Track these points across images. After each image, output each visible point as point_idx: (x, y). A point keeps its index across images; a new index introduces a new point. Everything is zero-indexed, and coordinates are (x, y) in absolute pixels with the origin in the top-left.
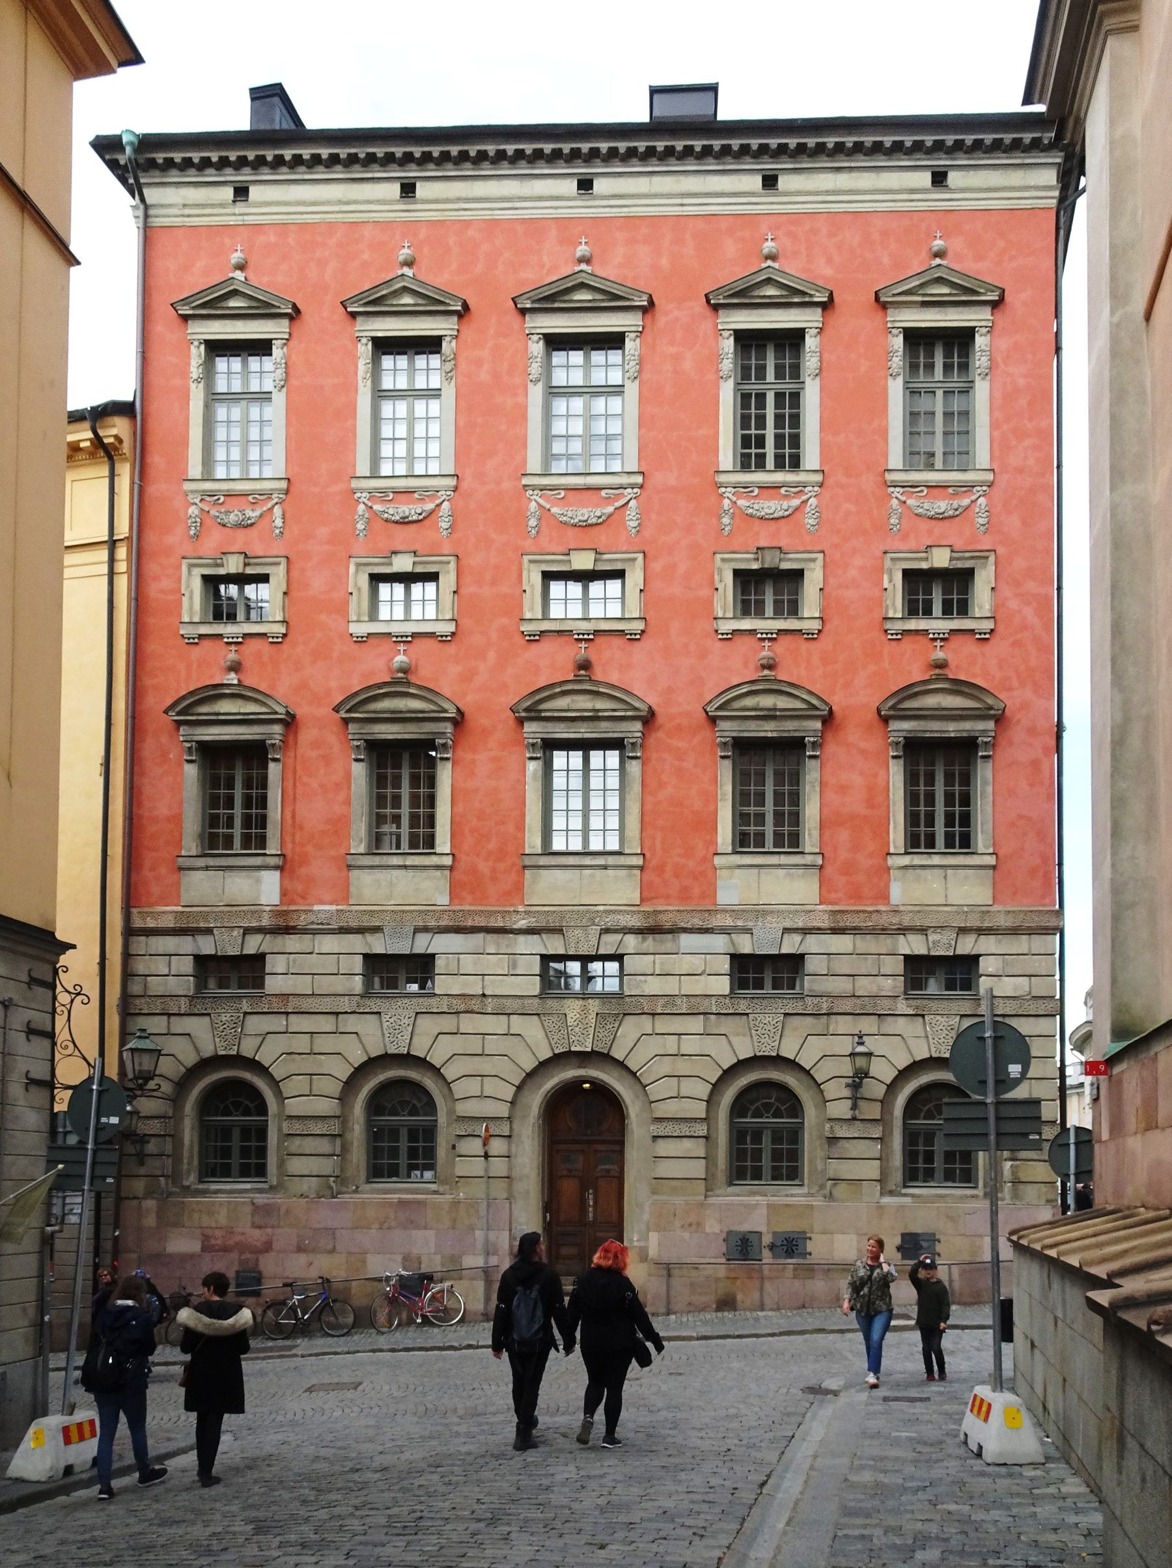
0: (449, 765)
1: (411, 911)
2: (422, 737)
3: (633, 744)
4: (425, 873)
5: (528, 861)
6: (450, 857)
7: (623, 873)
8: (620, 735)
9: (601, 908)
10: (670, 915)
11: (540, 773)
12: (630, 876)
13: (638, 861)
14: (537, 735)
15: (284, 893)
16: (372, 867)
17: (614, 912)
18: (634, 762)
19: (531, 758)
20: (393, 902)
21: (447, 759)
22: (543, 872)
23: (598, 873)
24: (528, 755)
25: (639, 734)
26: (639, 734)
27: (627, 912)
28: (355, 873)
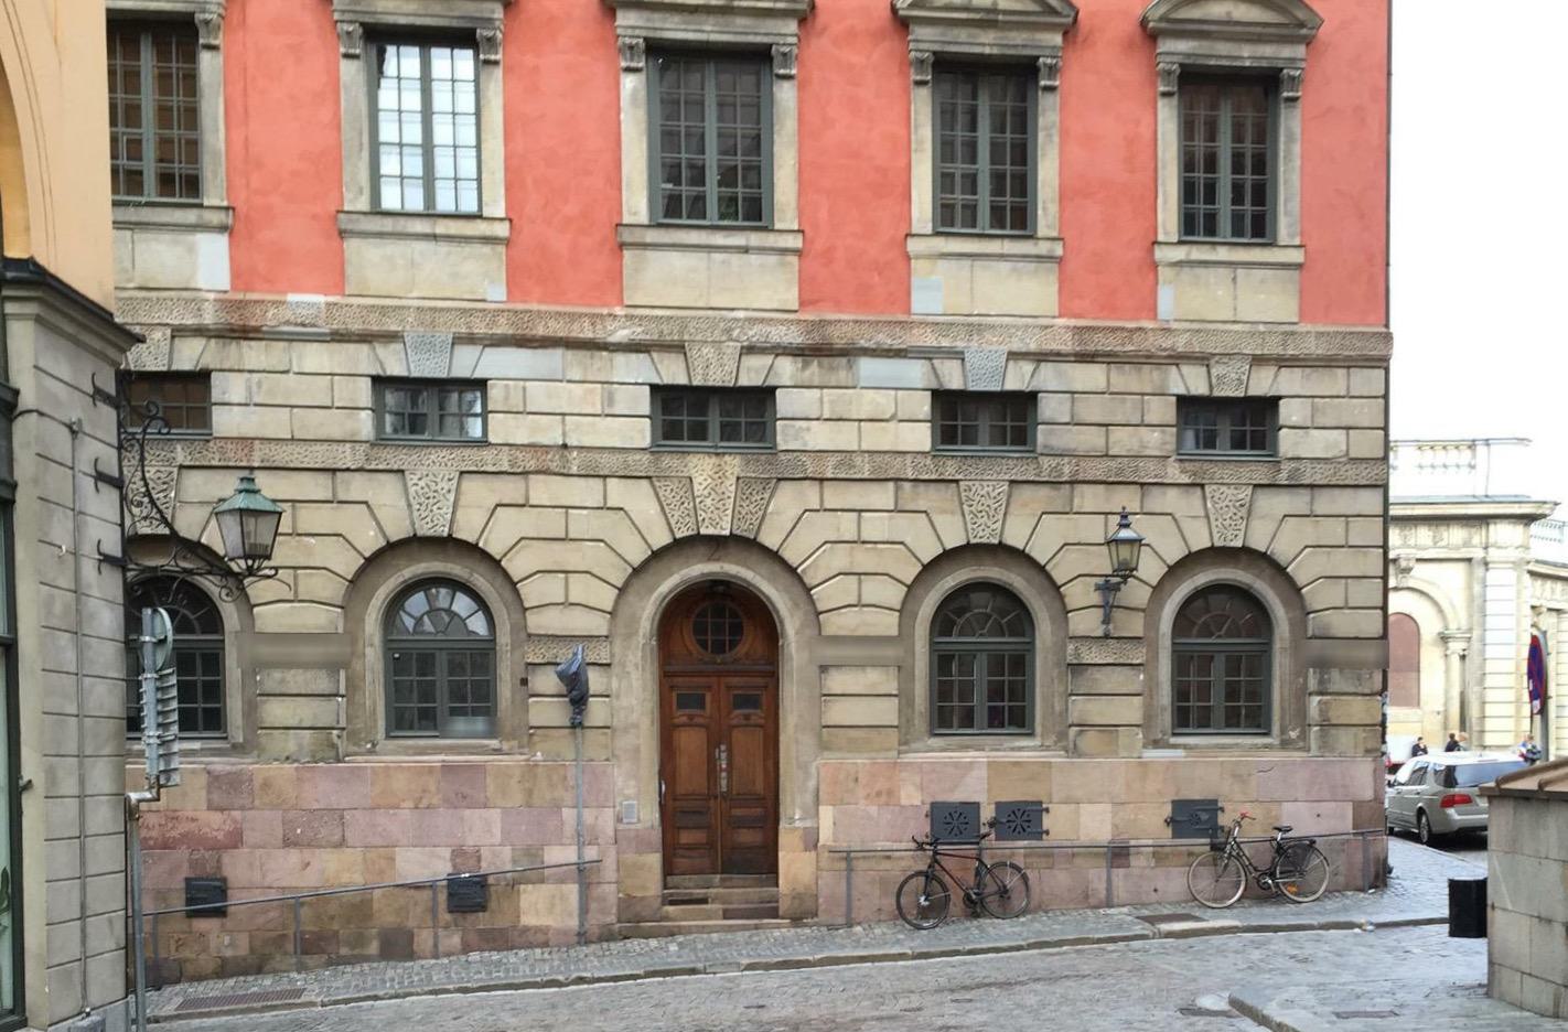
0: (498, 72)
1: (449, 310)
2: (455, 23)
3: (784, 54)
4: (468, 249)
5: (627, 236)
6: (506, 225)
7: (773, 259)
8: (766, 40)
9: (741, 314)
10: (845, 329)
11: (642, 94)
12: (783, 264)
13: (795, 242)
14: (637, 32)
15: (237, 274)
16: (381, 235)
17: (762, 321)
18: (786, 85)
19: (628, 70)
20: (415, 294)
21: (496, 63)
22: (651, 254)
23: (735, 259)
24: (624, 64)
25: (794, 40)
26: (794, 40)
27: (782, 322)
28: (352, 245)
